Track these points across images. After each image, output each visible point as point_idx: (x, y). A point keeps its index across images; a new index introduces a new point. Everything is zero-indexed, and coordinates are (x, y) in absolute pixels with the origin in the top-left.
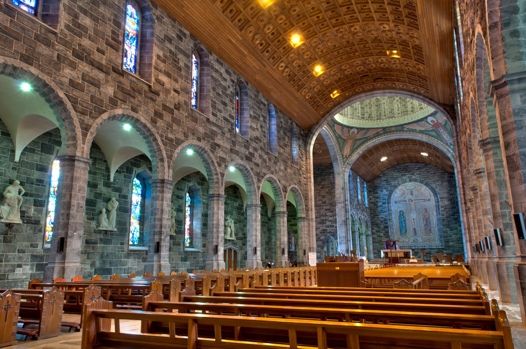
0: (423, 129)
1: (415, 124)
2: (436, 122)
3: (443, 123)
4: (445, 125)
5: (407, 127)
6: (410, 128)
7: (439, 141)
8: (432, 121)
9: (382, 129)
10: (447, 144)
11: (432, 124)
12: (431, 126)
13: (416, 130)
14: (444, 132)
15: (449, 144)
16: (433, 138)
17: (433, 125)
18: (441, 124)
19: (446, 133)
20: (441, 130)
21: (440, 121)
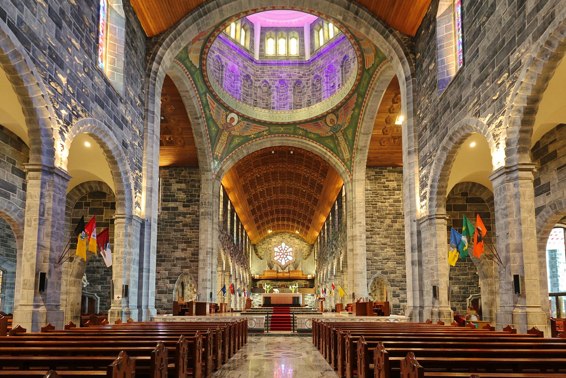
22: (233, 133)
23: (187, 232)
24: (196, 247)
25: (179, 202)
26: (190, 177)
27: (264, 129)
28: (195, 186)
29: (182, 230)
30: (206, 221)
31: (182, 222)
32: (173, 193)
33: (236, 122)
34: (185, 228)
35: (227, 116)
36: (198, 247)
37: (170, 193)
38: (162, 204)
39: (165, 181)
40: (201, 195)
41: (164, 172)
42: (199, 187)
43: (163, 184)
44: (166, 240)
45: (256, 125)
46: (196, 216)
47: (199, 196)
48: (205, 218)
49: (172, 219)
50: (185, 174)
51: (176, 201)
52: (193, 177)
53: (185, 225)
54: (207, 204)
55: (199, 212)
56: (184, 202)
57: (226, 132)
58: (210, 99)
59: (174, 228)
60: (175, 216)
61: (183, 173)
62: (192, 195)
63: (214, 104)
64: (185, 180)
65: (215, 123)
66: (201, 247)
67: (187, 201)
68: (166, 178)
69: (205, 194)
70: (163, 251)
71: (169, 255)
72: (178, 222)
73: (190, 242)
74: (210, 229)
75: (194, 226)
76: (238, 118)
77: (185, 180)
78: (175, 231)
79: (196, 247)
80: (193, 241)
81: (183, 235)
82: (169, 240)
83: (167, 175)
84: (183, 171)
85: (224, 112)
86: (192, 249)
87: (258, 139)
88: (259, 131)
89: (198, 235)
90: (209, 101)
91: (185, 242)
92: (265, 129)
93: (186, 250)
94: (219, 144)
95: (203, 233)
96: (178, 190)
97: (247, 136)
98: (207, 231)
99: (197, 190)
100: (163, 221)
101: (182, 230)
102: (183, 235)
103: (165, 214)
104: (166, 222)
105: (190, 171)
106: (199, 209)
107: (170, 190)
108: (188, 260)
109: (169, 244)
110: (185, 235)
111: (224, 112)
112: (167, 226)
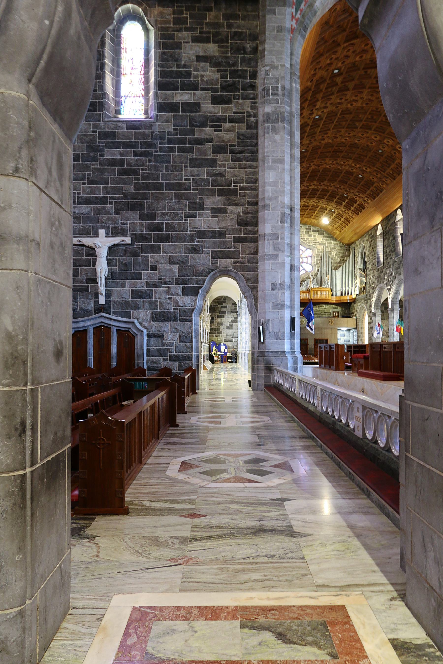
23: (224, 166)
24: (250, 204)
25: (203, 89)
26: (230, 26)
28: (244, 49)
29: (213, 162)
30: (277, 137)
31: (210, 140)
32: (185, 66)
34: (220, 157)
36: (256, 204)
37: (178, 66)
38: (156, 95)
39: (163, 37)
40: (261, 73)
41: (161, 13)
42: (255, 50)
43: (158, 45)
44: (170, 187)
46: (249, 127)
47: (254, 75)
48: (275, 130)
49: (185, 133)
50: (216, 17)
51: (194, 87)
52: (238, 27)
53: (219, 149)
54: (280, 92)
55: (255, 115)
56: (215, 90)
59: (190, 156)
60: (192, 125)
61: (211, 16)
62: (235, 74)
64: (216, 34)
66: (267, 202)
67: (224, 88)
68: (166, 29)
69: (274, 67)
70: (164, 214)
71: (180, 225)
72: (200, 142)
73: (234, 192)
74: (287, 159)
75: (242, 152)
77: (216, 34)
78: (194, 163)
79: (250, 204)
80: (242, 189)
81: (216, 175)
82: (179, 186)
83: (168, 22)
84: (210, 10)
86: (239, 209)
89: (256, 173)
91: (221, 193)
93: (222, 211)
95: (271, 168)
96: (199, 58)
98: (281, 161)
99: (250, 59)
100: (161, 138)
101: (213, 162)
102: (216, 175)
103: (167, 121)
104: (169, 141)
105: (229, 11)
106: (254, 107)
107: (177, 60)
108: (229, 238)
109: (178, 197)
110: (221, 175)
112: (171, 150)
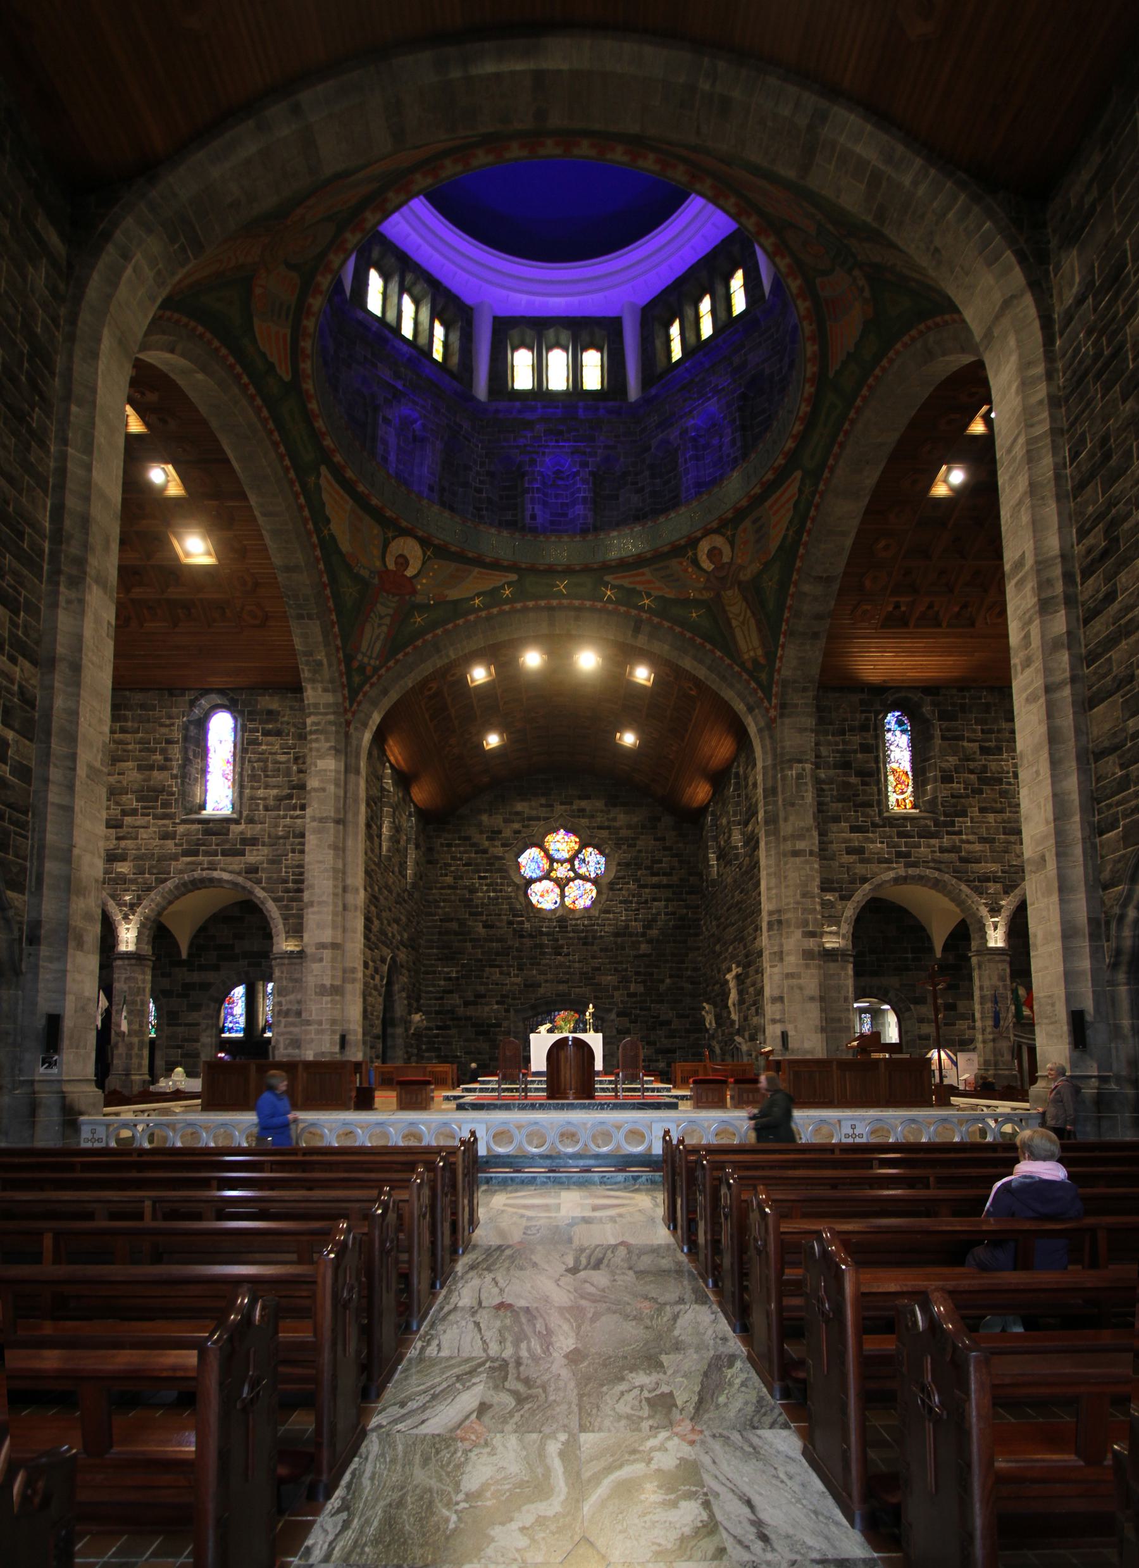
0: (345, 546)
1: (350, 504)
2: (409, 573)
3: (419, 599)
4: (423, 608)
5: (322, 482)
6: (325, 496)
7: (336, 629)
8: (403, 562)
9: (287, 378)
10: (349, 659)
11: (391, 566)
12: (378, 564)
13: (328, 521)
14: (387, 620)
15: (355, 664)
16: (331, 604)
17: (387, 571)
18: (414, 592)
19: (385, 629)
20: (385, 608)
21: (421, 584)
22: (746, 576)
27: (794, 488)
33: (726, 550)
35: (695, 562)
45: (774, 497)
57: (730, 593)
58: (624, 577)
63: (643, 574)
65: (686, 603)
76: (723, 535)
85: (681, 563)
87: (809, 524)
88: (791, 505)
90: (626, 583)
92: (796, 485)
94: (738, 634)
97: (781, 548)
111: (681, 563)
